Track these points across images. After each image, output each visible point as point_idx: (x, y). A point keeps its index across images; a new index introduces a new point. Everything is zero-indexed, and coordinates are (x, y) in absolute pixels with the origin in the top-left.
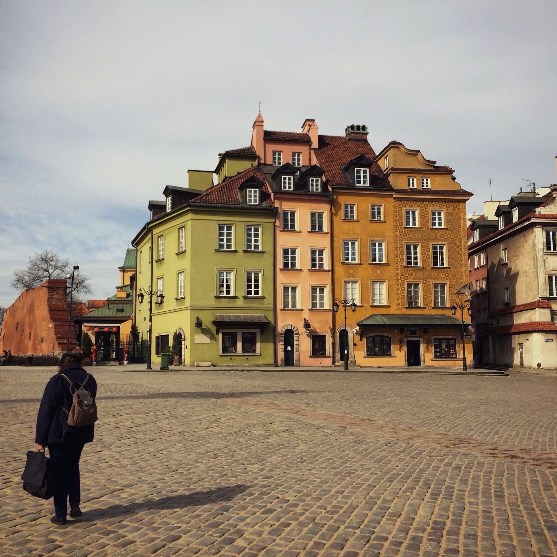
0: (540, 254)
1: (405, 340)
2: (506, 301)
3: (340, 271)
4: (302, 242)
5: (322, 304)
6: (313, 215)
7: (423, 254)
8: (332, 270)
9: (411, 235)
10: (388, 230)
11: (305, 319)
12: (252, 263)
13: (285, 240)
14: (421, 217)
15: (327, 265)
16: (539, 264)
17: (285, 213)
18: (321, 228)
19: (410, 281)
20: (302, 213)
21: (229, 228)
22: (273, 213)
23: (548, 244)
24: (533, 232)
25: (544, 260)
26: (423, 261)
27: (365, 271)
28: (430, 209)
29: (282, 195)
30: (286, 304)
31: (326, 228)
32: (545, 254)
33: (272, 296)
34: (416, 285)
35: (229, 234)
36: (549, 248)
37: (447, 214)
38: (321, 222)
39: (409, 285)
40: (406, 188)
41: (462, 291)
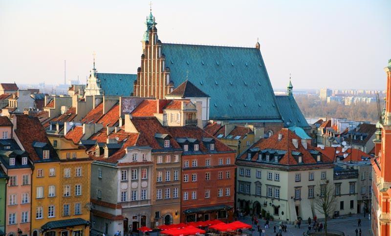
0: (119, 182)
1: (61, 232)
3: (35, 203)
5: (26, 220)
6: (24, 177)
8: (31, 203)
9: (67, 182)
11: (19, 229)
16: (119, 186)
17: (11, 177)
19: (65, 204)
20: (19, 175)
23: (123, 177)
24: (117, 172)
25: (121, 185)
26: (72, 193)
28: (76, 168)
30: (10, 222)
31: (29, 183)
32: (121, 182)
33: (4, 220)
34: (68, 206)
36: (123, 179)
37: (83, 170)
39: (65, 206)
41: (87, 206)
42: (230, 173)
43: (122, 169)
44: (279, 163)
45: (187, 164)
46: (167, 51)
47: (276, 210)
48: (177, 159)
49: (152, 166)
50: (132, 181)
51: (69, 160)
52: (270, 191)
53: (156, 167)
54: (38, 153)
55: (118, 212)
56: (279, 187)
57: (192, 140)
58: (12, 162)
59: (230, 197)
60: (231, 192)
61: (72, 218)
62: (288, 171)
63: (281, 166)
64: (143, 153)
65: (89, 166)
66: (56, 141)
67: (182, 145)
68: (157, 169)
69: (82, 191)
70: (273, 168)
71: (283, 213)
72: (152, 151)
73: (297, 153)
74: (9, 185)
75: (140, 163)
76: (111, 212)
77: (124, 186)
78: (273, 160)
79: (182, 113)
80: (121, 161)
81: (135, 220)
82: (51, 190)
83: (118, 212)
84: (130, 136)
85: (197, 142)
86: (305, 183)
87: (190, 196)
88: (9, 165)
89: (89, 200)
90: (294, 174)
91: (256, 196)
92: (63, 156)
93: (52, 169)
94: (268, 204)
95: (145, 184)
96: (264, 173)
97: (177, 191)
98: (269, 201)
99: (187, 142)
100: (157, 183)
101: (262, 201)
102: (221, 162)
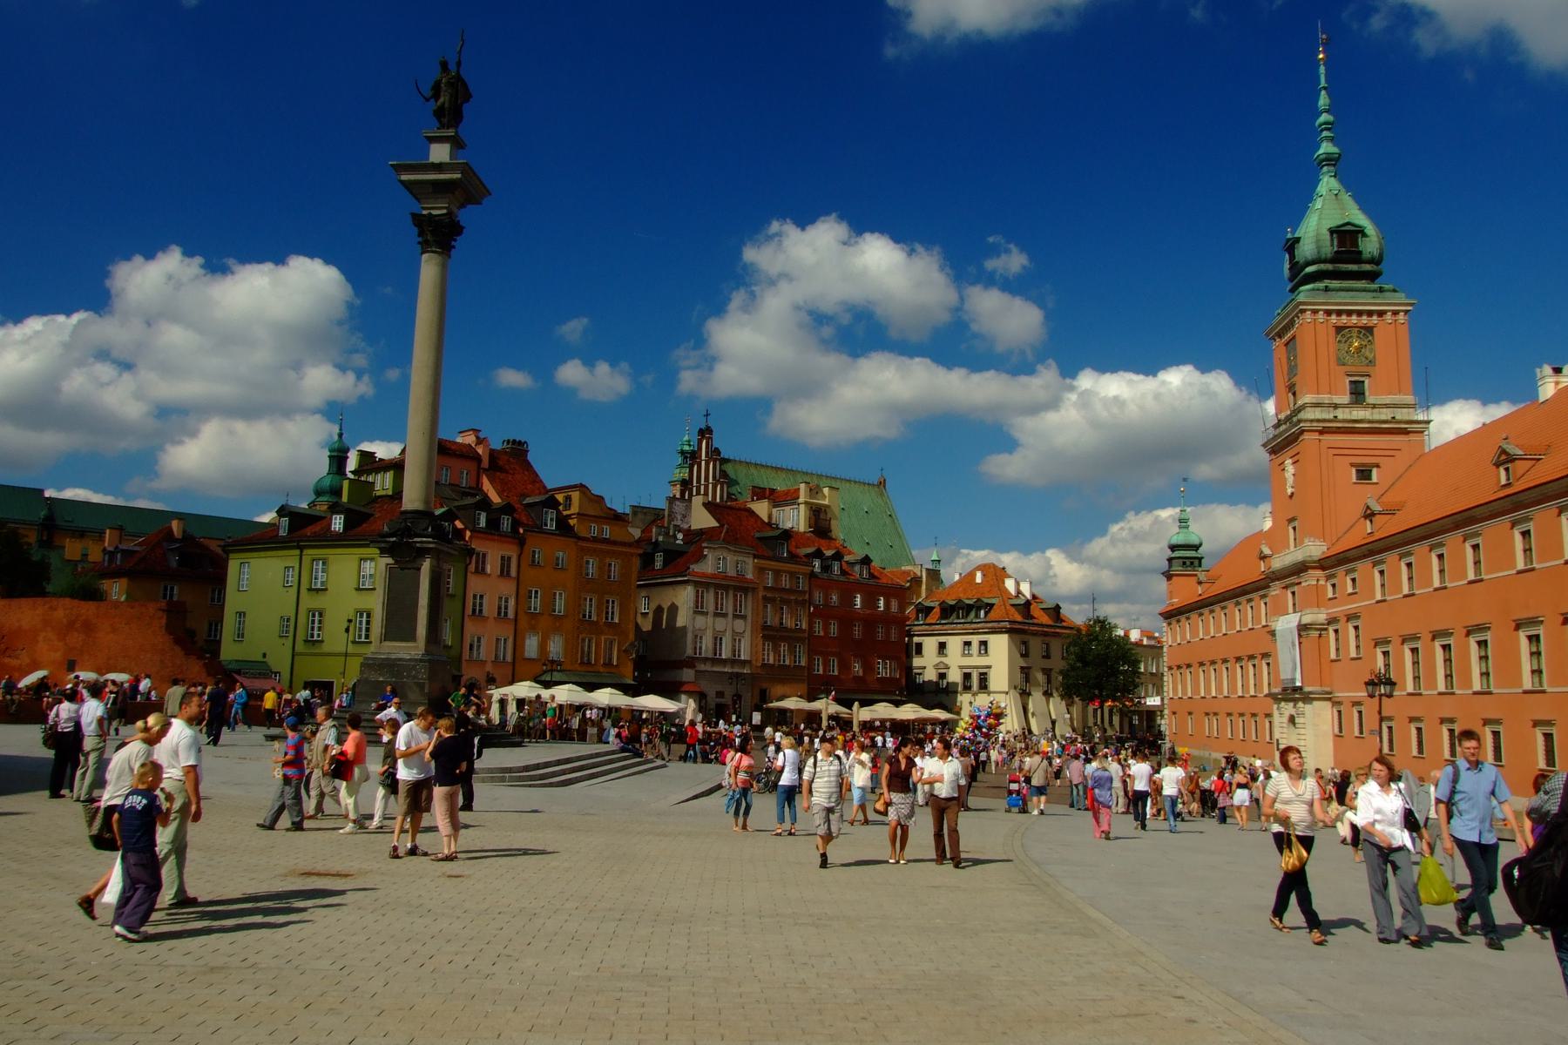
3: (523, 622)
13: (475, 584)
15: (511, 615)
20: (493, 553)
31: (513, 573)
32: (695, 612)
48: (803, 584)
50: (716, 615)
51: (595, 540)
53: (761, 594)
55: (687, 675)
57: (829, 553)
65: (636, 563)
66: (568, 498)
72: (755, 557)
73: (1021, 601)
74: (472, 567)
77: (700, 621)
78: (973, 614)
79: (802, 507)
82: (560, 605)
84: (702, 532)
85: (838, 556)
90: (1018, 637)
93: (563, 552)
95: (739, 625)
96: (955, 644)
99: (818, 554)
100: (765, 627)
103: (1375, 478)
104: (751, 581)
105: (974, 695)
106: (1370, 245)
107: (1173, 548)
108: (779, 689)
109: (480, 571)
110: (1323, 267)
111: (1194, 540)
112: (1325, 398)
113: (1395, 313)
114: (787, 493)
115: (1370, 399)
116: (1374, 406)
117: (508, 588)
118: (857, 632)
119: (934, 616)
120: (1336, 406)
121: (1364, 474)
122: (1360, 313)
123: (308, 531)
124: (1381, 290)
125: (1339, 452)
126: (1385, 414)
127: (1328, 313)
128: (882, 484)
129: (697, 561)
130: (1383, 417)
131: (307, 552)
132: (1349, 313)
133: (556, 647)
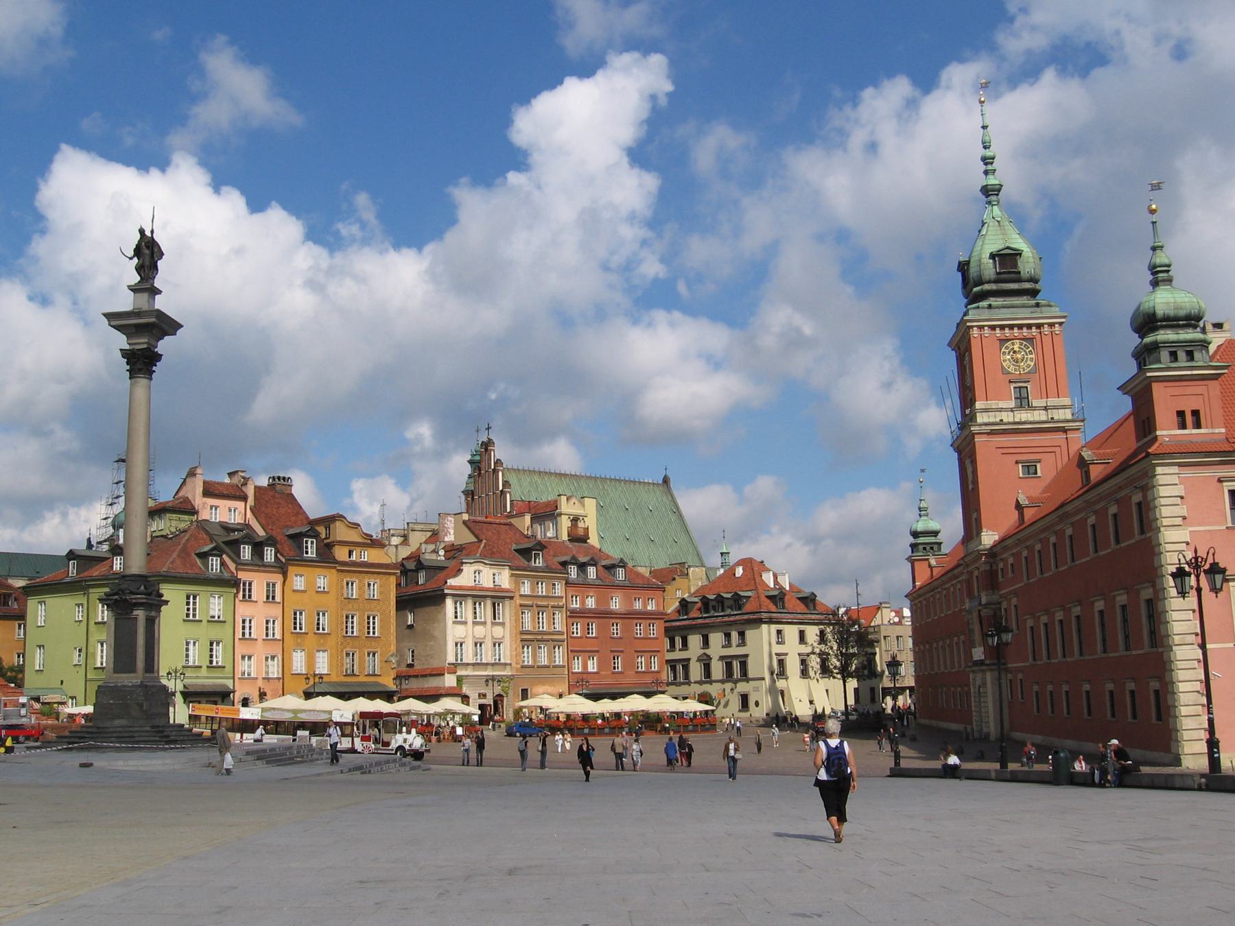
2: (410, 661)
4: (257, 613)
6: (268, 585)
7: (359, 623)
10: (331, 601)
12: (215, 632)
13: (243, 610)
14: (360, 588)
18: (273, 598)
20: (258, 582)
21: (195, 598)
22: (234, 583)
26: (360, 631)
27: (311, 640)
29: (240, 565)
35: (194, 603)
38: (274, 591)
39: (348, 655)
40: (347, 559)
42: (656, 630)
43: (453, 595)
44: (744, 611)
45: (576, 605)
46: (513, 480)
47: (745, 698)
48: (559, 589)
49: (511, 598)
50: (475, 623)
51: (354, 564)
52: (729, 666)
53: (519, 601)
54: (297, 538)
55: (450, 681)
56: (747, 656)
57: (583, 559)
58: (246, 552)
59: (658, 672)
60: (660, 666)
61: (362, 679)
62: (760, 621)
63: (746, 617)
64: (492, 571)
65: (393, 580)
67: (564, 564)
68: (521, 605)
69: (381, 627)
70: (731, 624)
71: (757, 704)
72: (511, 568)
73: (776, 593)
75: (488, 590)
76: (433, 683)
80: (451, 582)
81: (483, 701)
83: (450, 681)
86: (792, 649)
87: (585, 666)
88: (239, 556)
89: (393, 648)
91: (700, 683)
92: (341, 554)
94: (728, 691)
95: (498, 632)
97: (560, 657)
98: (728, 686)
99: (574, 561)
100: (522, 633)
101: (713, 690)
102: (638, 606)
103: (1039, 474)
104: (507, 591)
105: (736, 682)
106: (1028, 263)
107: (915, 534)
108: (540, 689)
109: (248, 598)
110: (987, 287)
111: (933, 525)
112: (993, 404)
113: (1051, 325)
114: (548, 504)
115: (1035, 403)
116: (1035, 408)
117: (276, 611)
118: (616, 630)
119: (694, 613)
120: (1000, 410)
121: (1030, 468)
122: (1020, 327)
123: (96, 571)
124: (1038, 305)
125: (1005, 451)
126: (1040, 416)
127: (993, 328)
128: (666, 481)
129: (455, 576)
130: (1044, 418)
131: (91, 590)
132: (1011, 327)
133: (323, 664)
